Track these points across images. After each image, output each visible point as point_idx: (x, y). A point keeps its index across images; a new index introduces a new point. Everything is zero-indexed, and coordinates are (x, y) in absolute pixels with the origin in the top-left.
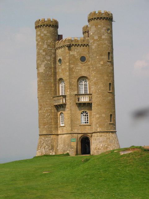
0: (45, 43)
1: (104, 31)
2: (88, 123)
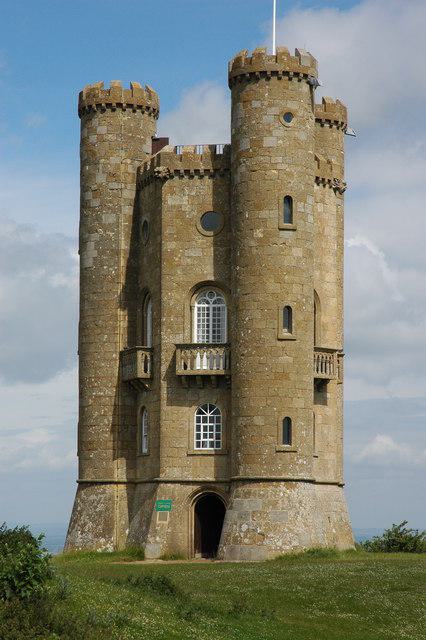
0: (100, 167)
1: (272, 118)
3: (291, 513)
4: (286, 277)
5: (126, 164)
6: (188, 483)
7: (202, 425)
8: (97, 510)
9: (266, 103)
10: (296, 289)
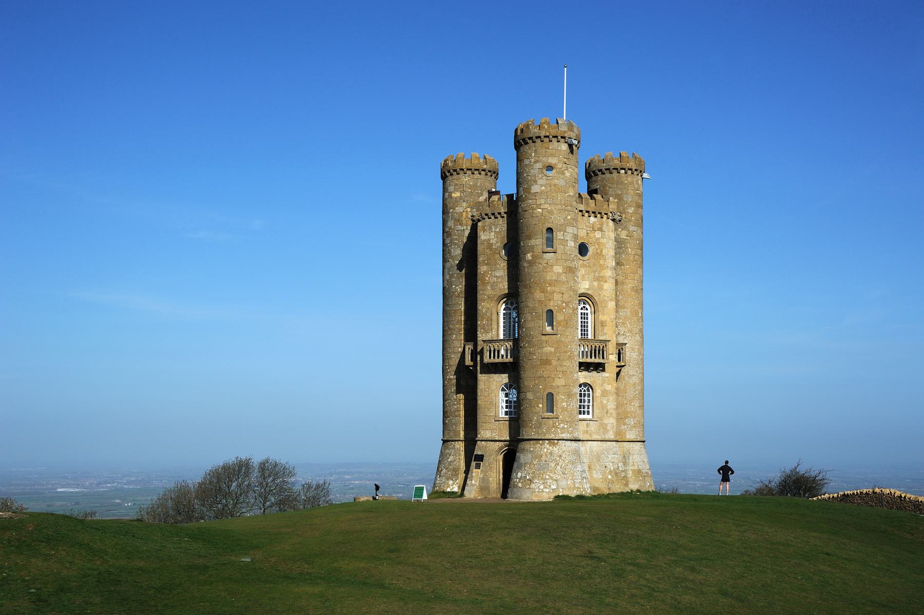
3: (553, 465)
4: (549, 288)
5: (467, 211)
8: (449, 460)
9: (533, 160)
10: (557, 297)
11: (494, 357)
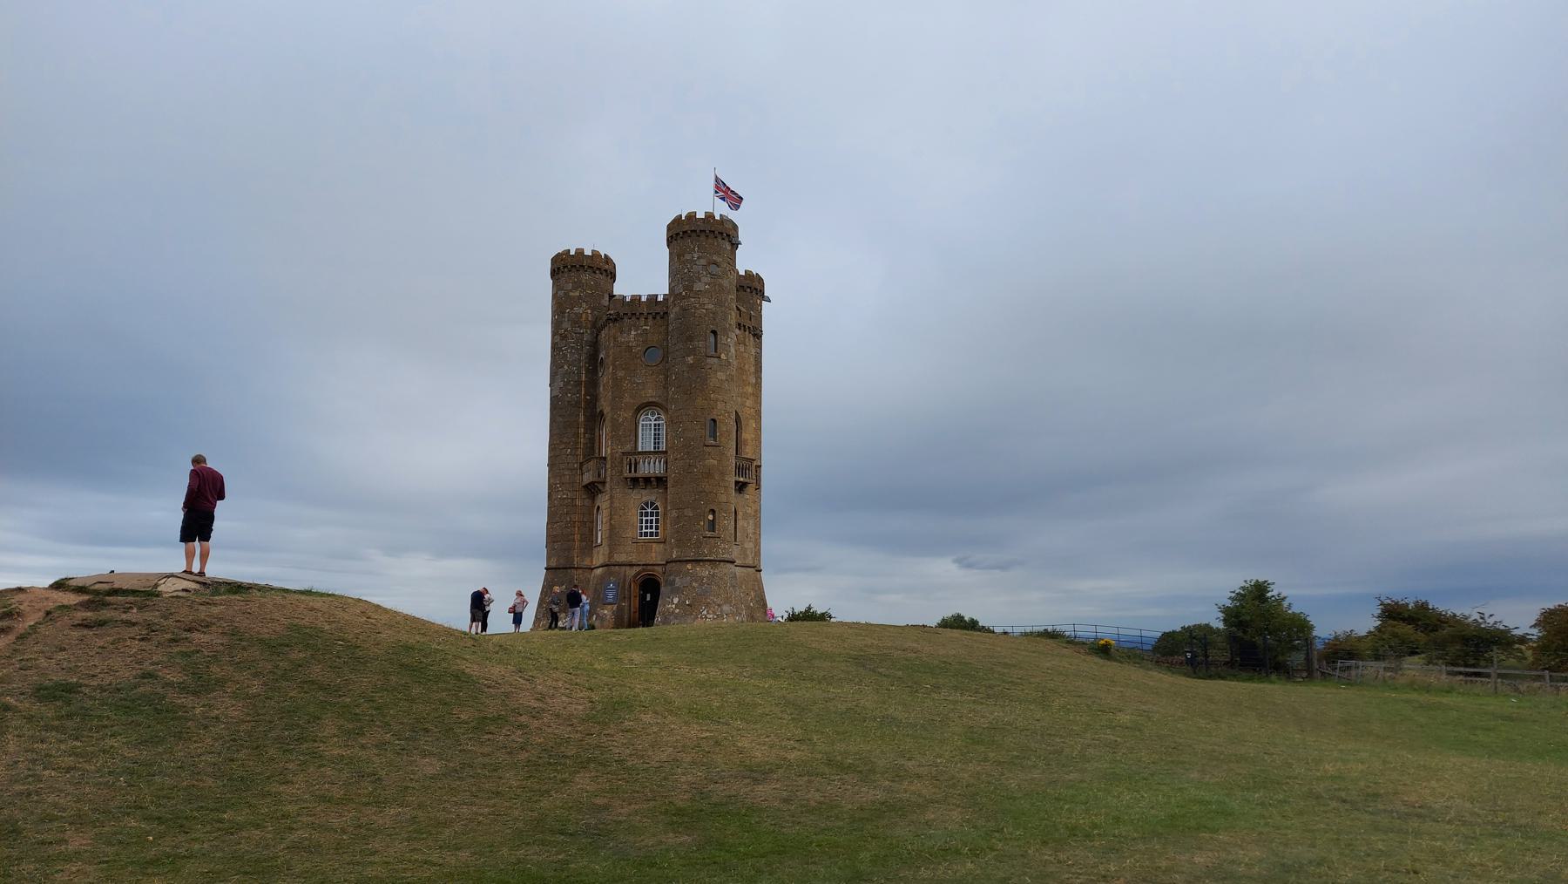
2: (657, 534)
4: (712, 396)
6: (631, 565)
7: (644, 518)
9: (696, 256)
10: (720, 405)
11: (635, 471)
